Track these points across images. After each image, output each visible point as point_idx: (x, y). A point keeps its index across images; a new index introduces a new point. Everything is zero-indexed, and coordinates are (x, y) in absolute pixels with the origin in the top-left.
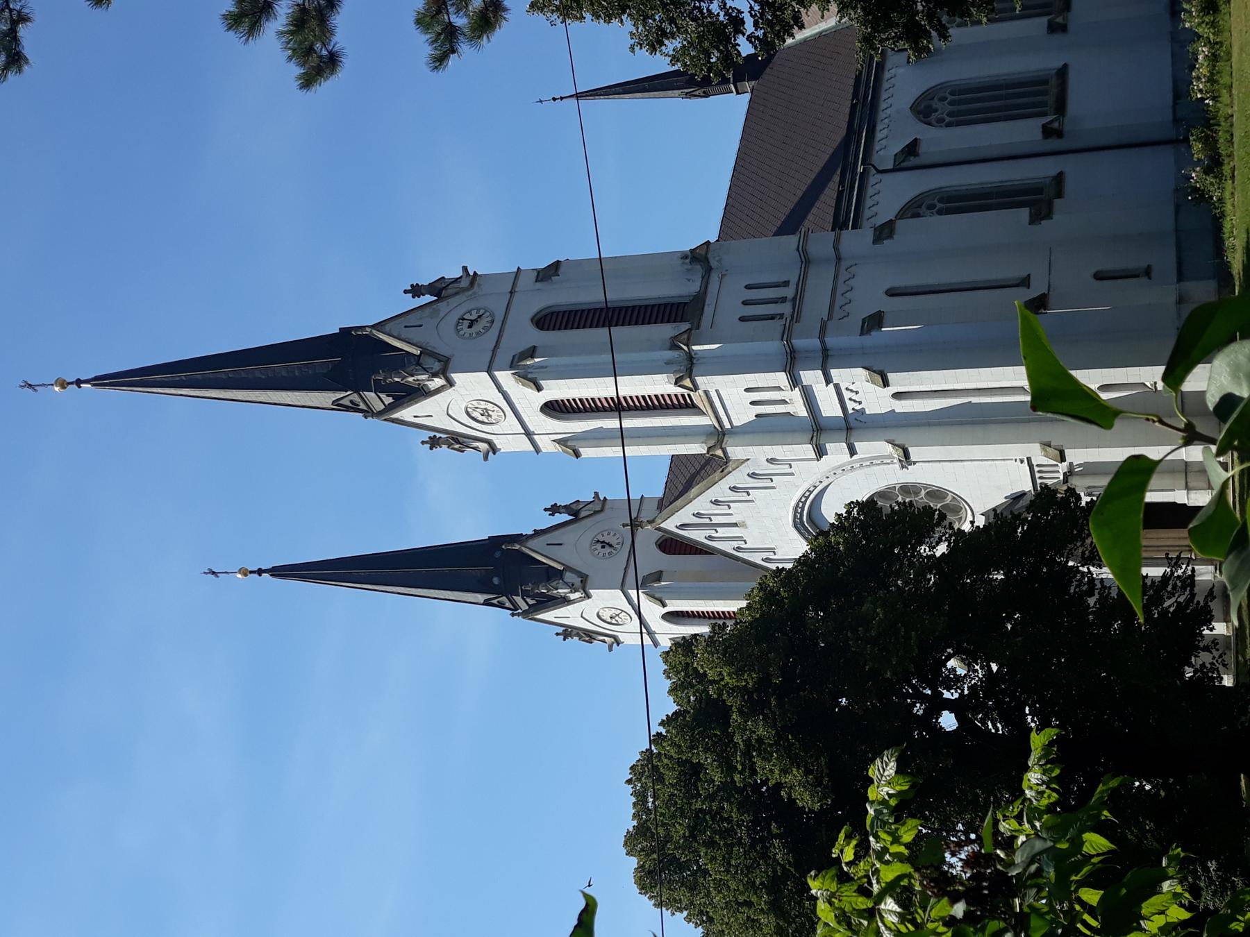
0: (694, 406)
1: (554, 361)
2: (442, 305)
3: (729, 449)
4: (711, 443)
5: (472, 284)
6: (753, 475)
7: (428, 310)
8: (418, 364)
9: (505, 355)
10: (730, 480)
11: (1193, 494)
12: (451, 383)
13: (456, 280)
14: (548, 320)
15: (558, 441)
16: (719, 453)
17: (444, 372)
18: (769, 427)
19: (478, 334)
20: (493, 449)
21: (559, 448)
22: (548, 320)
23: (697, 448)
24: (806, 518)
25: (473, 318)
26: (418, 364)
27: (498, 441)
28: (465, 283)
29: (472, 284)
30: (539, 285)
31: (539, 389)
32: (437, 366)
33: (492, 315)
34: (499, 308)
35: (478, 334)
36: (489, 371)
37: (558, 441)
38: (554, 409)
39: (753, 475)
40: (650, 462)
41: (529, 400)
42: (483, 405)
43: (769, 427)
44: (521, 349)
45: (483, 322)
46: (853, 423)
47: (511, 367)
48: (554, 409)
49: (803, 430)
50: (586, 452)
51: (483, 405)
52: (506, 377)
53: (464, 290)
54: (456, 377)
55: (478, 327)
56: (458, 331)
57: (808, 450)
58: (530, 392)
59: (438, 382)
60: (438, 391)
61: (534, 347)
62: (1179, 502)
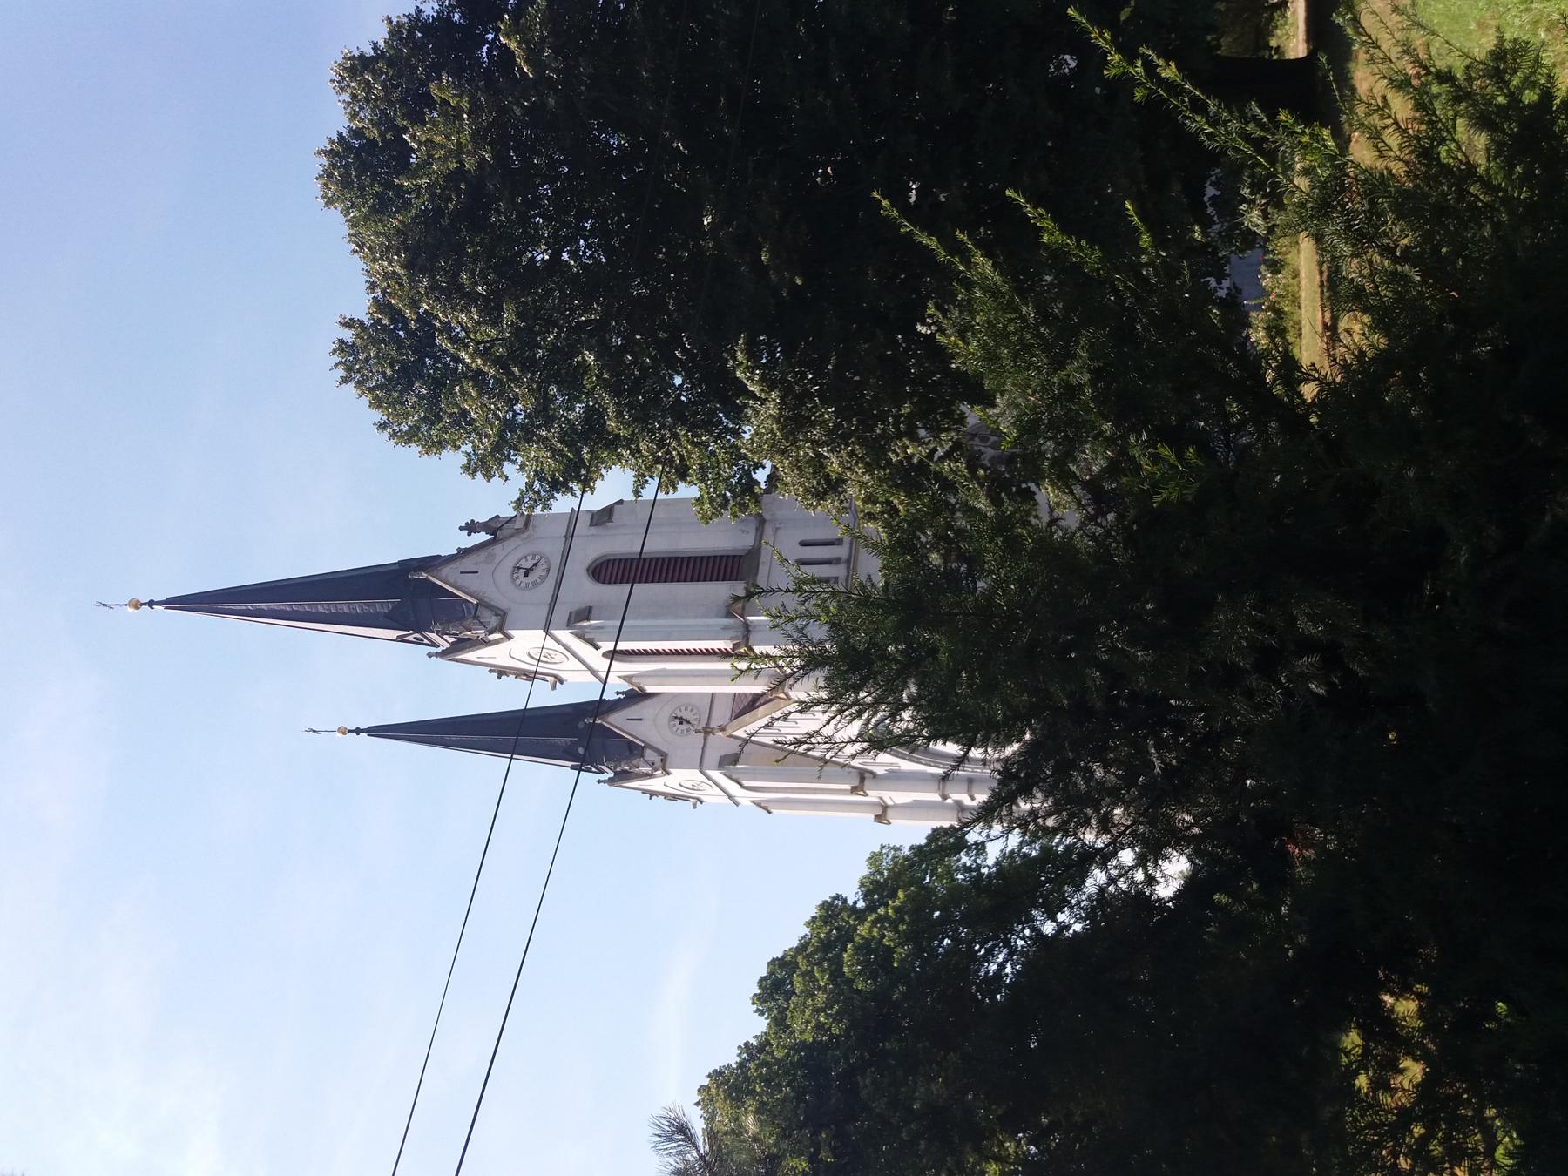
2: (497, 548)
5: (526, 525)
7: (483, 555)
8: (476, 617)
9: (561, 613)
12: (509, 638)
14: (605, 571)
15: (624, 678)
17: (500, 628)
19: (535, 584)
22: (605, 571)
26: (476, 617)
27: (562, 675)
28: (519, 524)
29: (526, 525)
30: (593, 530)
31: (597, 648)
32: (494, 621)
33: (548, 562)
34: (553, 550)
35: (535, 584)
37: (624, 678)
44: (577, 607)
45: (539, 572)
47: (569, 626)
52: (565, 635)
54: (511, 632)
55: (533, 577)
56: (514, 580)
59: (498, 636)
60: (497, 642)
61: (590, 609)
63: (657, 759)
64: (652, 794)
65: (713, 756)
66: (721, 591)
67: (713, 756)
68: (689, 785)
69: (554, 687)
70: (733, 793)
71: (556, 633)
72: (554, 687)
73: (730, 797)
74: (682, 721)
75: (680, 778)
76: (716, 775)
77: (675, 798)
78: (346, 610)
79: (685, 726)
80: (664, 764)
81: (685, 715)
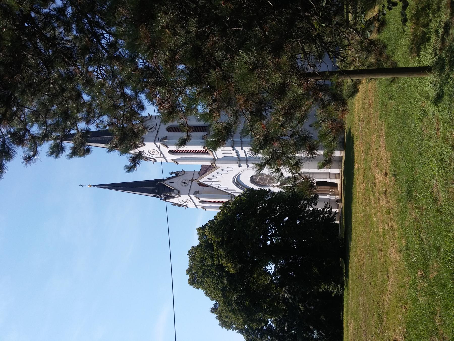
0: (208, 153)
1: (171, 140)
3: (217, 164)
4: (212, 162)
5: (151, 118)
6: (223, 170)
10: (217, 171)
11: (331, 180)
12: (144, 145)
13: (146, 117)
15: (173, 160)
16: (214, 165)
18: (227, 159)
19: (152, 132)
20: (156, 161)
21: (172, 162)
23: (209, 163)
24: (237, 182)
25: (151, 127)
28: (149, 118)
29: (151, 118)
31: (168, 148)
35: (152, 132)
36: (154, 142)
37: (173, 160)
38: (171, 152)
39: (223, 170)
40: (196, 166)
41: (165, 150)
42: (153, 150)
43: (227, 159)
46: (248, 159)
47: (160, 142)
48: (171, 152)
49: (236, 160)
50: (179, 163)
51: (153, 150)
53: (148, 120)
54: (145, 143)
55: (152, 130)
57: (237, 165)
58: (165, 148)
62: (328, 181)
63: (177, 192)
64: (174, 204)
65: (192, 191)
66: (201, 134)
67: (192, 191)
68: (185, 201)
69: (154, 163)
70: (196, 204)
71: (157, 143)
72: (154, 163)
73: (196, 205)
74: (184, 183)
75: (183, 198)
76: (193, 197)
77: (180, 205)
78: (100, 139)
79: (185, 184)
80: (179, 193)
81: (185, 182)
